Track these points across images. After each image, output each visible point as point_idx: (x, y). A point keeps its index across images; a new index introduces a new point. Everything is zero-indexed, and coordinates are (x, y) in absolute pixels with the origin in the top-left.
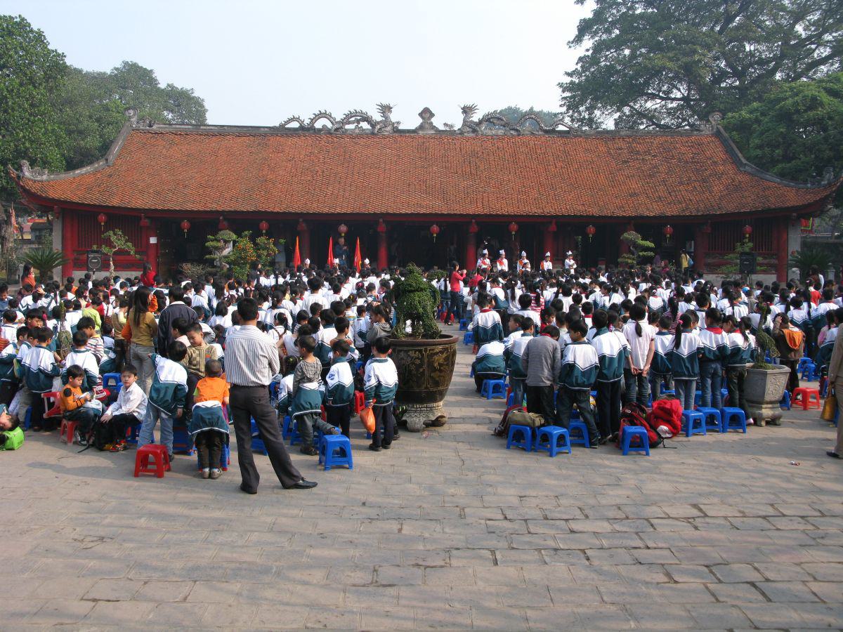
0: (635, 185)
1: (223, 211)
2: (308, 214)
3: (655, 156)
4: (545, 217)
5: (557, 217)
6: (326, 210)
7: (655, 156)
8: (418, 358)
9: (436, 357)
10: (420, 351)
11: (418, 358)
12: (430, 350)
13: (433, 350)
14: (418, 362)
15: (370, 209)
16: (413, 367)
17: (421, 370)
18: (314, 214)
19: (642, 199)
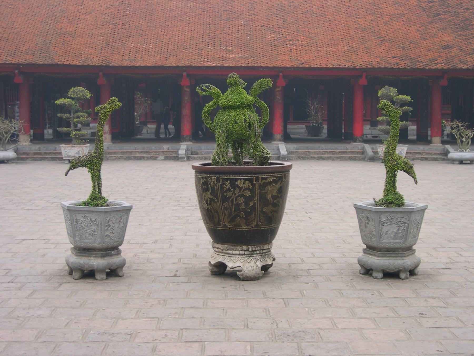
0: (447, 38)
1: (18, 65)
2: (107, 67)
3: (468, 9)
4: (354, 69)
5: (366, 70)
6: (126, 63)
7: (468, 9)
8: (248, 189)
9: (269, 188)
10: (251, 180)
11: (248, 189)
12: (262, 179)
13: (266, 179)
14: (247, 193)
15: (172, 62)
16: (241, 200)
17: (252, 204)
18: (114, 67)
19: (455, 51)
